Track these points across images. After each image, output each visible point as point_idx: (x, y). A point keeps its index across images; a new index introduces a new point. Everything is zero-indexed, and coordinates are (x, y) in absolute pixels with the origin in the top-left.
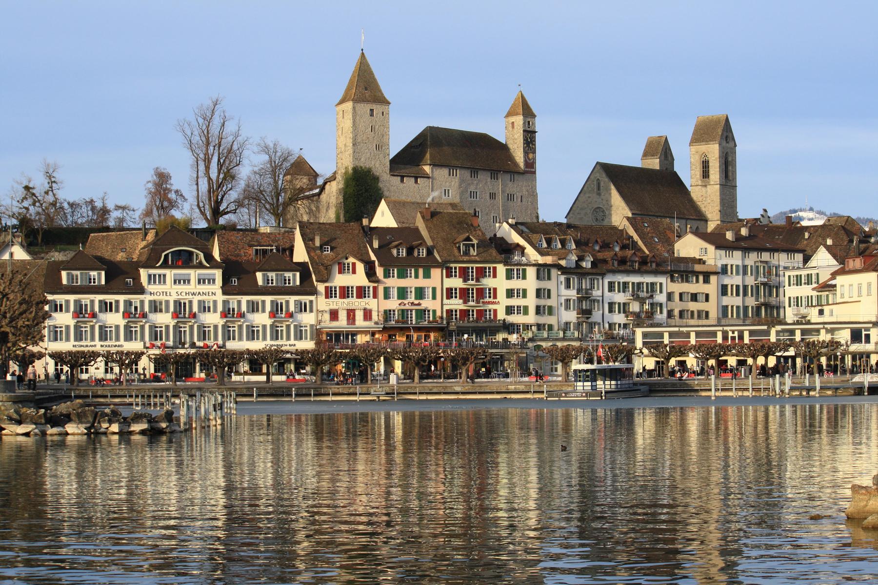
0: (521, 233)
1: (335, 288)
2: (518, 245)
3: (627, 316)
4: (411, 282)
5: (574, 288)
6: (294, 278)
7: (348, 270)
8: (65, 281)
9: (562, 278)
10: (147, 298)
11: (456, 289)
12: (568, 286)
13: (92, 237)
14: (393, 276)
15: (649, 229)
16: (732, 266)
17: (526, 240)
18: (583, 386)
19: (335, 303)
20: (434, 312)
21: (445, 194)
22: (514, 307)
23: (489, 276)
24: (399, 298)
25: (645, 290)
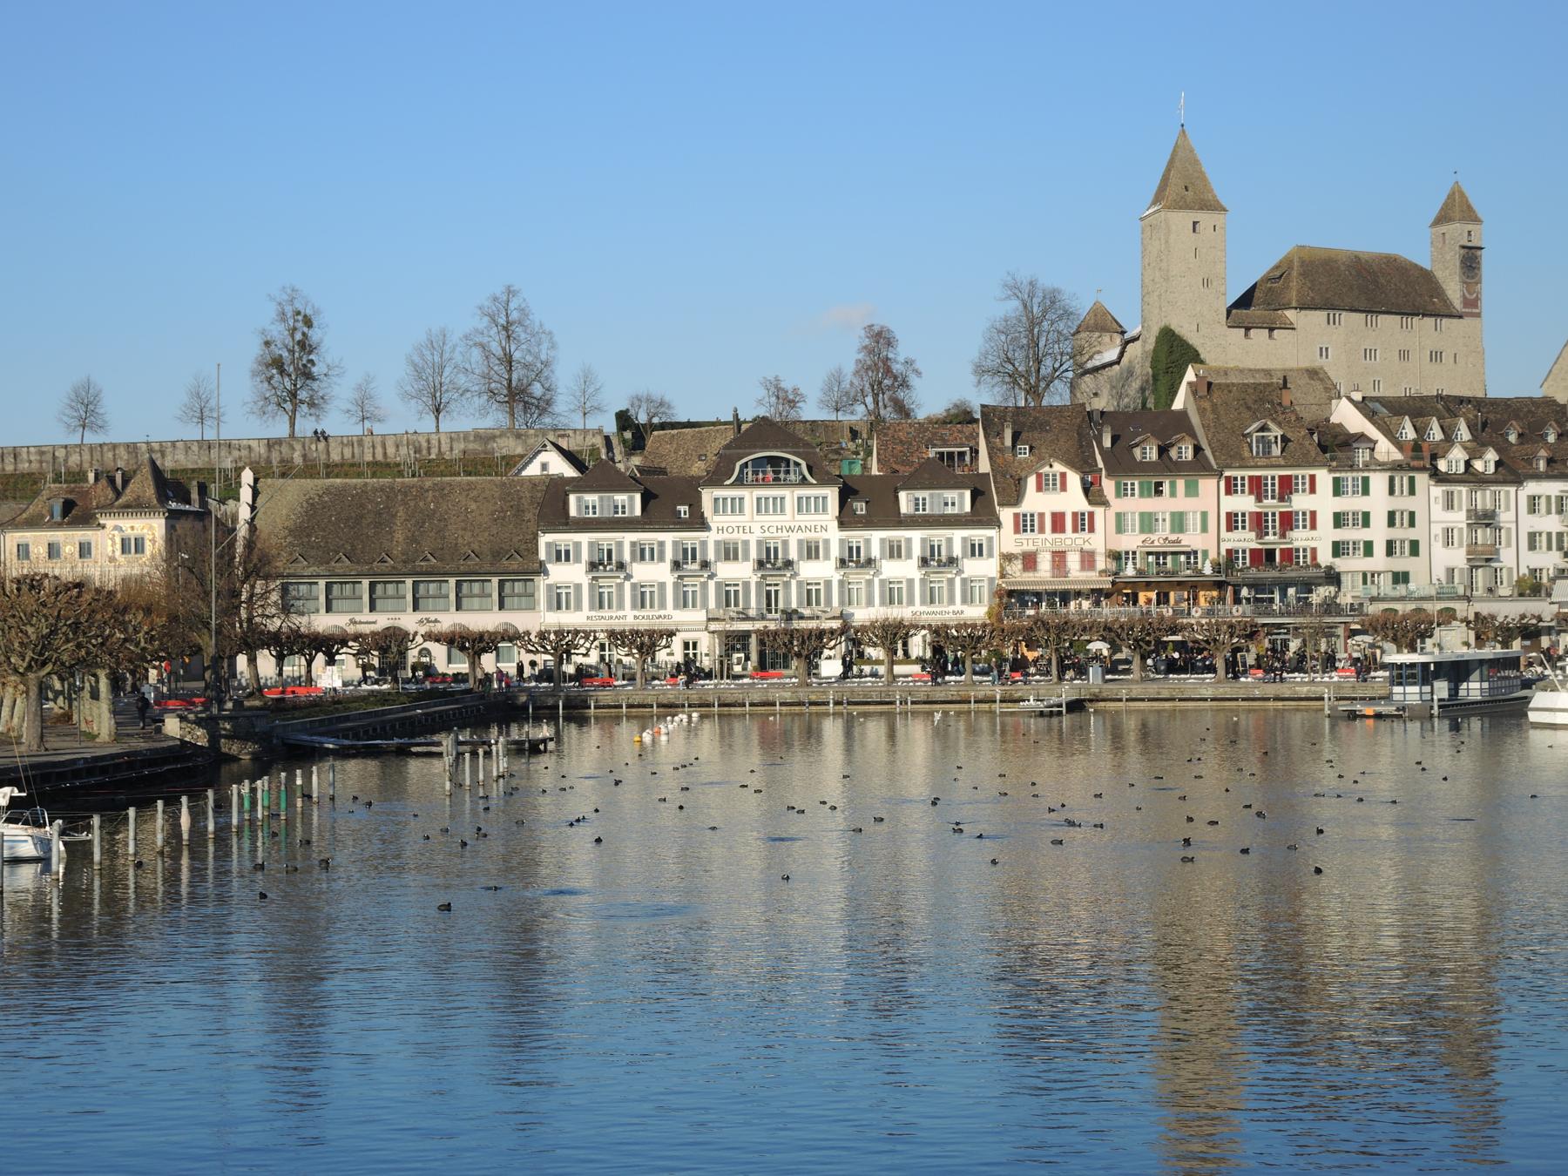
0: (1371, 415)
1: (1032, 515)
2: (1362, 437)
4: (1163, 506)
6: (961, 500)
7: (1054, 484)
8: (573, 512)
9: (1438, 491)
10: (711, 537)
11: (1243, 515)
12: (1449, 505)
13: (655, 437)
14: (1133, 495)
17: (1379, 428)
19: (1031, 542)
20: (1205, 553)
21: (1321, 355)
22: (1348, 543)
23: (1304, 491)
24: (1142, 531)
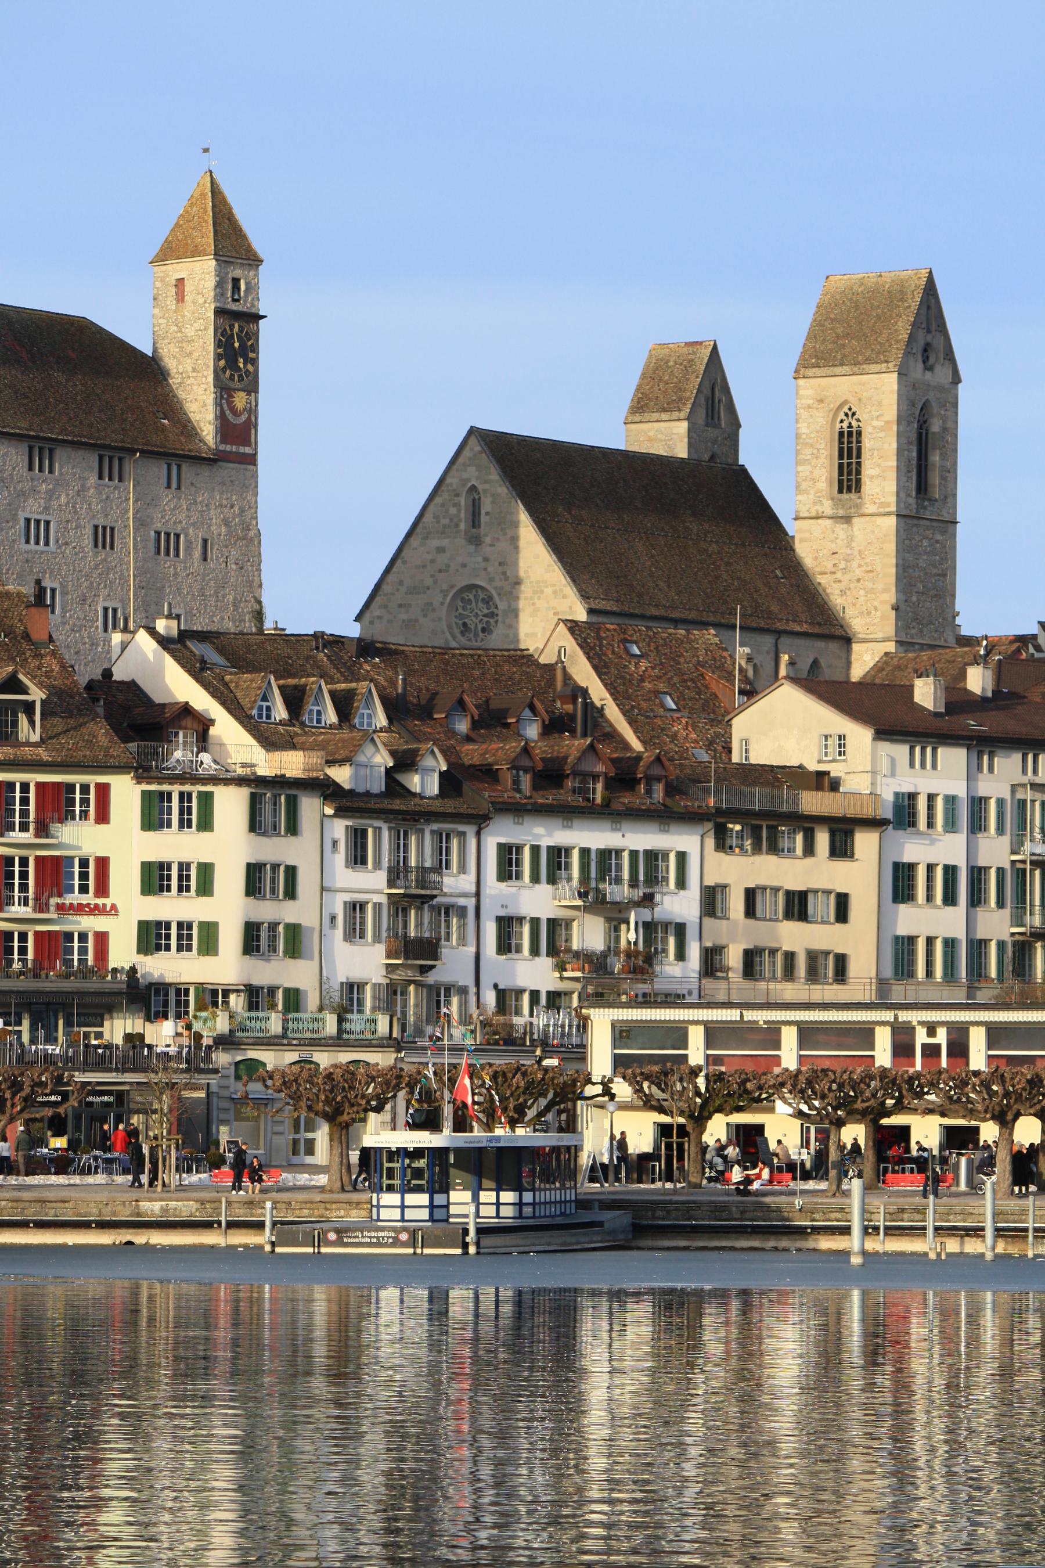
0: (197, 670)
2: (186, 710)
3: (561, 967)
5: (377, 865)
9: (339, 829)
12: (358, 858)
15: (644, 664)
16: (931, 798)
18: (403, 1207)
25: (626, 875)
